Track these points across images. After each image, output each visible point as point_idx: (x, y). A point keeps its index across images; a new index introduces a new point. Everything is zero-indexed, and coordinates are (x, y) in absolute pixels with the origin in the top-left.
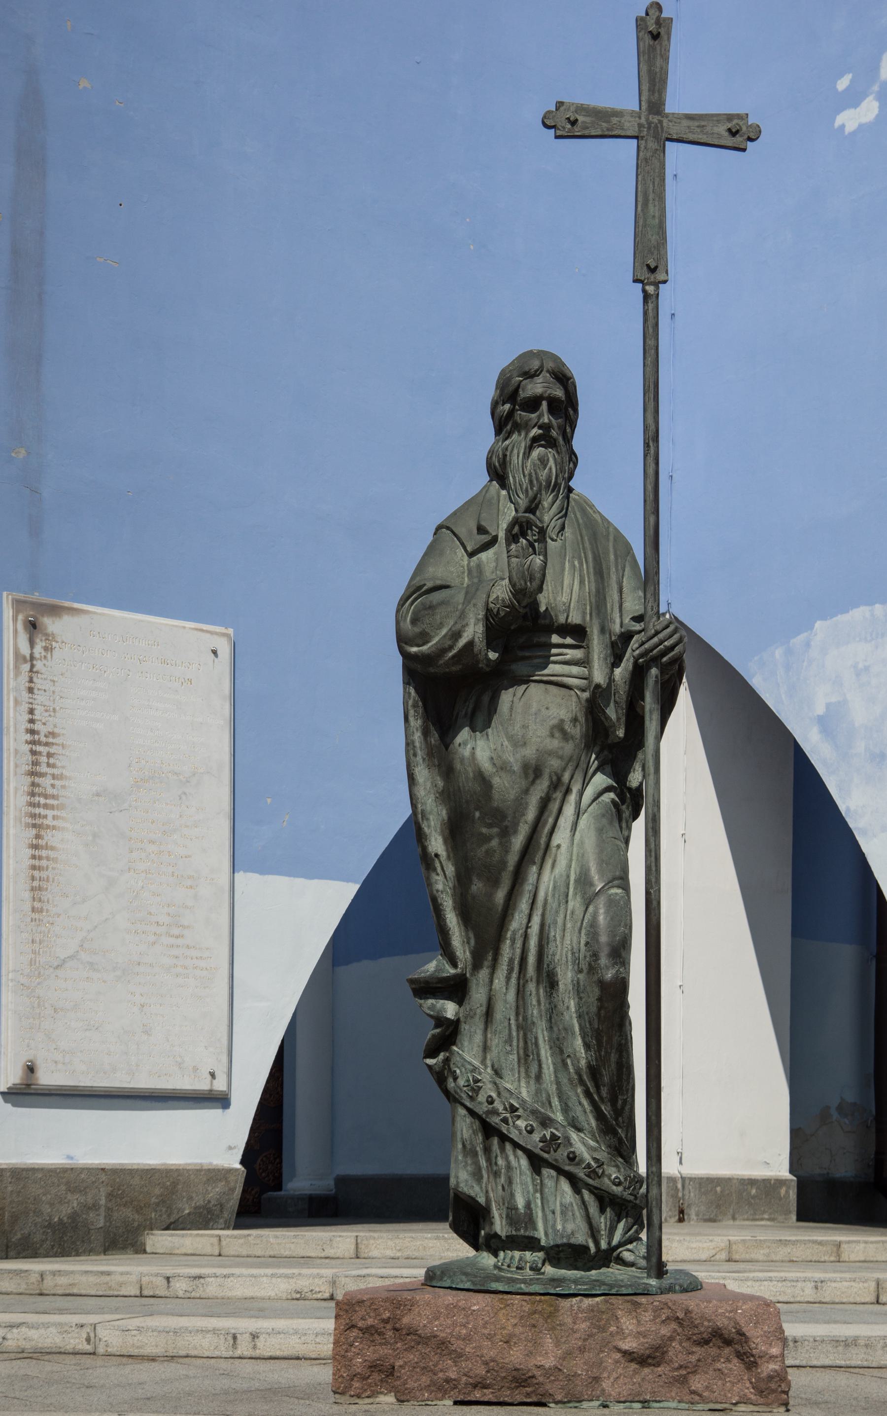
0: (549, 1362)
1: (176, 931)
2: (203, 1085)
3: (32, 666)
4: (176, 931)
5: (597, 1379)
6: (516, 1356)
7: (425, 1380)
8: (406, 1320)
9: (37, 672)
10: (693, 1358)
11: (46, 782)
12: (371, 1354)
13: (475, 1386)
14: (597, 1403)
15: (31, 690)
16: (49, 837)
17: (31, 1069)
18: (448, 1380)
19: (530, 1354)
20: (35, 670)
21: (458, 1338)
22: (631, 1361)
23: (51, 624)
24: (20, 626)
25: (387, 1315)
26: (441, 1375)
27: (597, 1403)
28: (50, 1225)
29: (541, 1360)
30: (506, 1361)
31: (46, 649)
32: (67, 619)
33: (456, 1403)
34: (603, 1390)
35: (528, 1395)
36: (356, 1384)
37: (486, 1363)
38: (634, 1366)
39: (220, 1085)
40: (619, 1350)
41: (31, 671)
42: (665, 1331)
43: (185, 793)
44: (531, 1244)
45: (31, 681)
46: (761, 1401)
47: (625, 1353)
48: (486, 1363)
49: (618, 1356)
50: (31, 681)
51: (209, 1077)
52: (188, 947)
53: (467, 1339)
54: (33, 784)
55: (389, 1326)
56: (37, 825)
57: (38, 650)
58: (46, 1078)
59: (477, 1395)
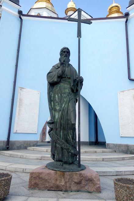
0: (63, 184)
2: (34, 133)
5: (70, 187)
7: (43, 186)
8: (41, 176)
10: (86, 183)
11: (21, 104)
12: (35, 181)
13: (51, 187)
14: (70, 191)
16: (21, 109)
18: (47, 186)
19: (60, 182)
21: (49, 179)
23: (23, 90)
25: (37, 175)
26: (45, 185)
27: (70, 191)
28: (17, 146)
32: (24, 89)
33: (48, 190)
34: (71, 189)
35: (59, 189)
36: (32, 187)
38: (76, 184)
42: (81, 178)
44: (61, 161)
46: (97, 191)
47: (75, 183)
49: (73, 182)
53: (50, 179)
55: (38, 177)
56: (20, 107)
58: (18, 132)
59: (51, 189)
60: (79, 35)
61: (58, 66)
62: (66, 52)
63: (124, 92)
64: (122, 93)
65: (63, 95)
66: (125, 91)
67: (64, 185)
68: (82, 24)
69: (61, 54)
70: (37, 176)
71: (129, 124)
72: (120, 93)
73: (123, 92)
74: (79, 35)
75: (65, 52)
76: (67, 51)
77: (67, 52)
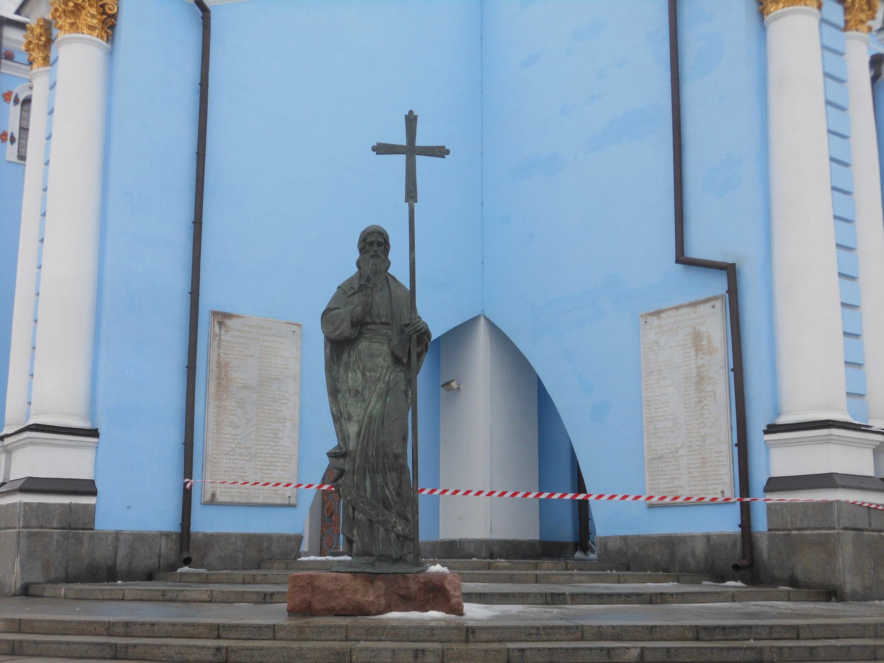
0: (371, 598)
1: (276, 440)
3: (220, 338)
4: (276, 440)
6: (358, 597)
9: (222, 340)
15: (219, 347)
17: (214, 495)
19: (364, 596)
20: (221, 339)
22: (403, 599)
23: (228, 322)
24: (216, 323)
29: (367, 599)
30: (354, 599)
31: (226, 331)
37: (346, 600)
39: (293, 501)
40: (399, 595)
41: (220, 339)
43: (281, 386)
44: (371, 555)
45: (219, 343)
48: (346, 600)
49: (397, 597)
50: (219, 343)
51: (288, 498)
52: (280, 446)
54: (219, 383)
57: (223, 332)
60: (411, 195)
61: (352, 288)
62: (375, 244)
63: (662, 315)
64: (655, 321)
65: (368, 374)
66: (667, 310)
67: (373, 601)
68: (419, 159)
69: (362, 250)
70: (308, 584)
71: (677, 452)
72: (649, 319)
73: (657, 313)
74: (411, 195)
75: (371, 244)
76: (381, 240)
77: (379, 244)
